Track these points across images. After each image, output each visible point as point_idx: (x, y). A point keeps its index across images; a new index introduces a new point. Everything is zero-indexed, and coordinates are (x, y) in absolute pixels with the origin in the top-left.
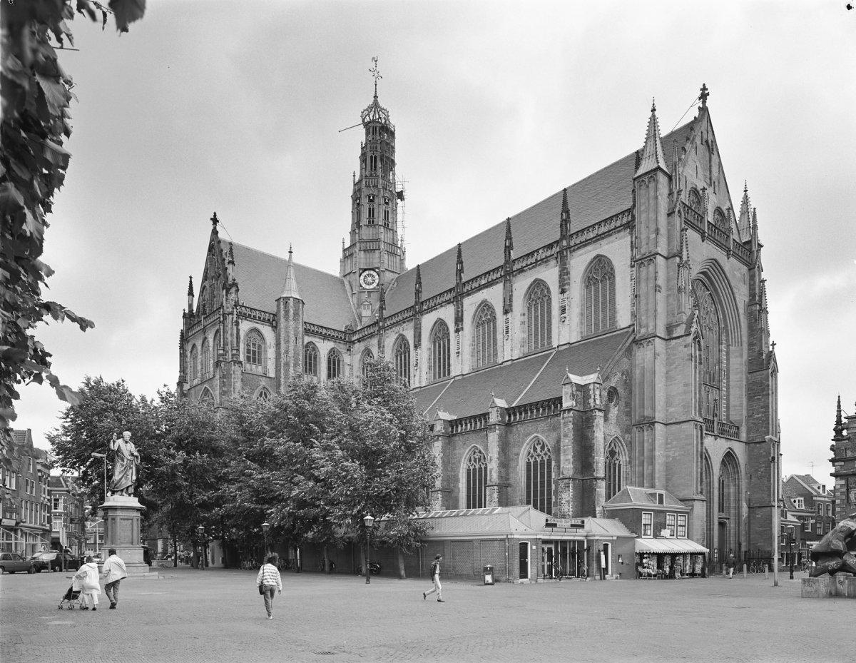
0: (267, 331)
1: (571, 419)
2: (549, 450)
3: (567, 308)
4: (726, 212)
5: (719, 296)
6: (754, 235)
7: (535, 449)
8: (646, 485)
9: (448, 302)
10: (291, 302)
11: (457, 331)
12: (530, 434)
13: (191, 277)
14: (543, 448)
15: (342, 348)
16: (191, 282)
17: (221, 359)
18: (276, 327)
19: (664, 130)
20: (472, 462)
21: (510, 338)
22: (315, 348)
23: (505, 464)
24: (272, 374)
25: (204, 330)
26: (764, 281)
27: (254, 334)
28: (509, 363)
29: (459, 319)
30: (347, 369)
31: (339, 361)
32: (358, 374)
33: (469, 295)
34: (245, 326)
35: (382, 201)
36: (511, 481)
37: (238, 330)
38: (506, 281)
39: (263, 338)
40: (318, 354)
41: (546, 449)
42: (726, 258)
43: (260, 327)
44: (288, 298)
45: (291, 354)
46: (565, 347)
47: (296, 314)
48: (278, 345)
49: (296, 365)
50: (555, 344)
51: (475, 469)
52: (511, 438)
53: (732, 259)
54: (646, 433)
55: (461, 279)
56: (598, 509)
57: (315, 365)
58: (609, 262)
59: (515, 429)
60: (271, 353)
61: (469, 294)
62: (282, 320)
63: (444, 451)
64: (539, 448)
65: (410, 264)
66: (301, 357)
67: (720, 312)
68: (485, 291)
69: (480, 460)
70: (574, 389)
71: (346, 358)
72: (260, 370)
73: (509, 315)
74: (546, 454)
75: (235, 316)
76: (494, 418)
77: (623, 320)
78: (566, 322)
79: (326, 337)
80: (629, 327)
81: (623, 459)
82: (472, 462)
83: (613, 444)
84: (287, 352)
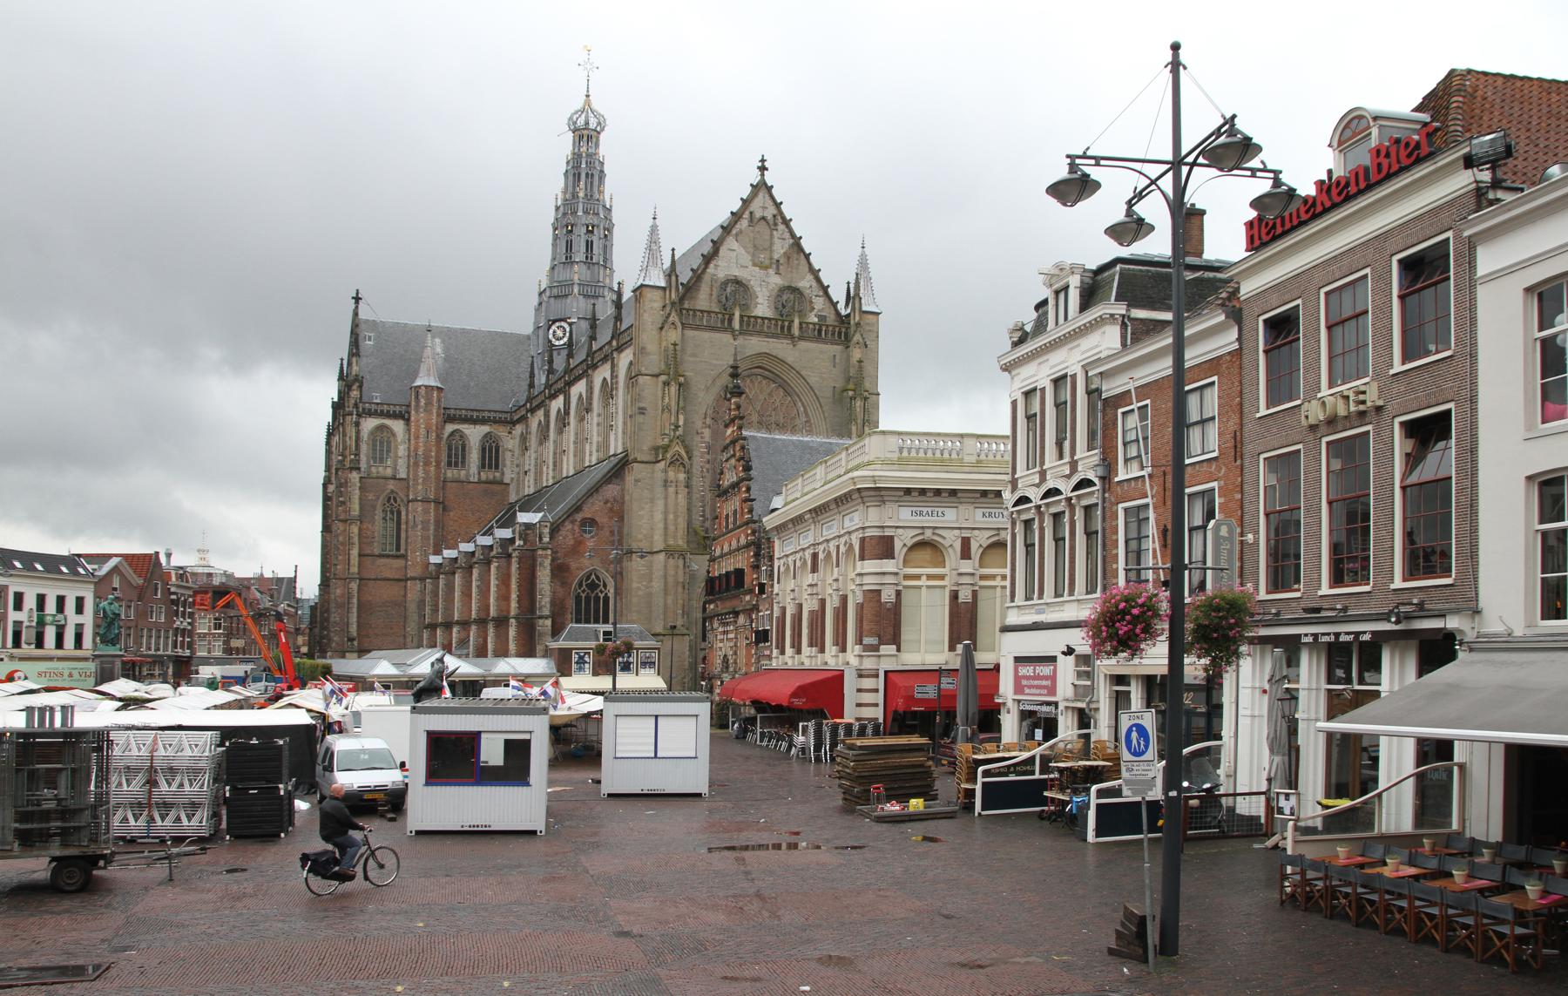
0: (397, 426)
10: (422, 391)
15: (501, 431)
22: (462, 436)
34: (369, 424)
35: (584, 230)
37: (358, 433)
39: (394, 435)
43: (388, 422)
47: (429, 403)
49: (427, 464)
53: (803, 345)
57: (464, 457)
60: (402, 451)
72: (389, 472)
84: (416, 449)
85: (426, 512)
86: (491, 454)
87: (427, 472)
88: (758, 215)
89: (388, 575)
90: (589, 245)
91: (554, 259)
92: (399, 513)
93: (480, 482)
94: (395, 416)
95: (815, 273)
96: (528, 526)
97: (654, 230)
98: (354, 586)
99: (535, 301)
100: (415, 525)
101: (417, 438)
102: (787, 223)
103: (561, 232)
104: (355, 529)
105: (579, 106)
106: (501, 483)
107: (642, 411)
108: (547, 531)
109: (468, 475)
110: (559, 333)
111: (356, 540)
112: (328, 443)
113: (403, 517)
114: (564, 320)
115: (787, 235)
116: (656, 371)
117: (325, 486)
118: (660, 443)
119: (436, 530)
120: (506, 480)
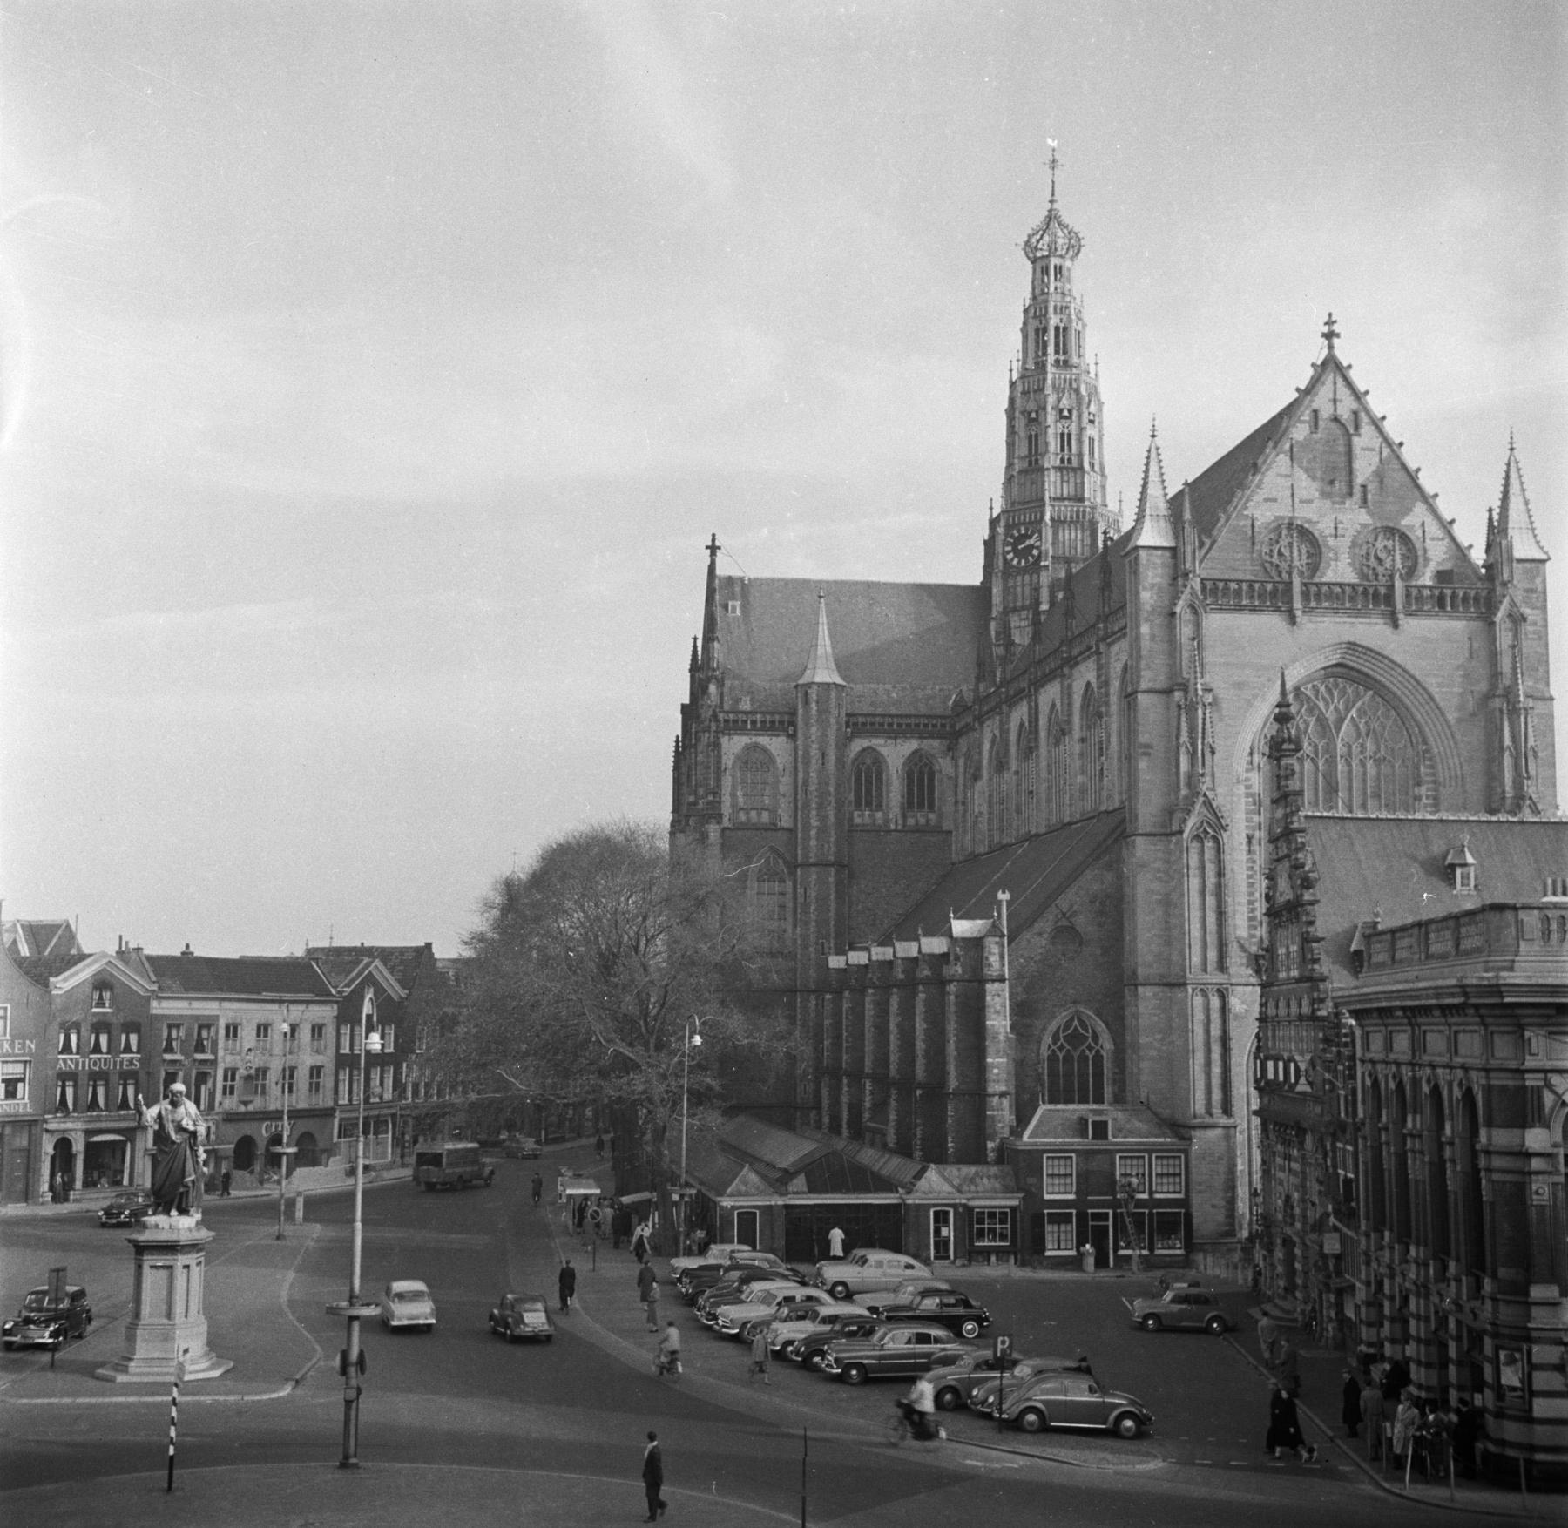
0: (777, 745)
13: (695, 639)
16: (695, 647)
22: (879, 761)
34: (733, 745)
39: (772, 759)
42: (1388, 630)
43: (763, 740)
49: (820, 806)
53: (1410, 625)
56: (990, 1145)
57: (879, 789)
66: (831, 789)
83: (1076, 1023)
84: (806, 782)
87: (823, 818)
88: (1326, 412)
91: (1010, 466)
93: (906, 830)
94: (771, 728)
95: (1428, 501)
102: (1377, 424)
103: (1020, 424)
106: (938, 830)
109: (887, 821)
115: (1377, 442)
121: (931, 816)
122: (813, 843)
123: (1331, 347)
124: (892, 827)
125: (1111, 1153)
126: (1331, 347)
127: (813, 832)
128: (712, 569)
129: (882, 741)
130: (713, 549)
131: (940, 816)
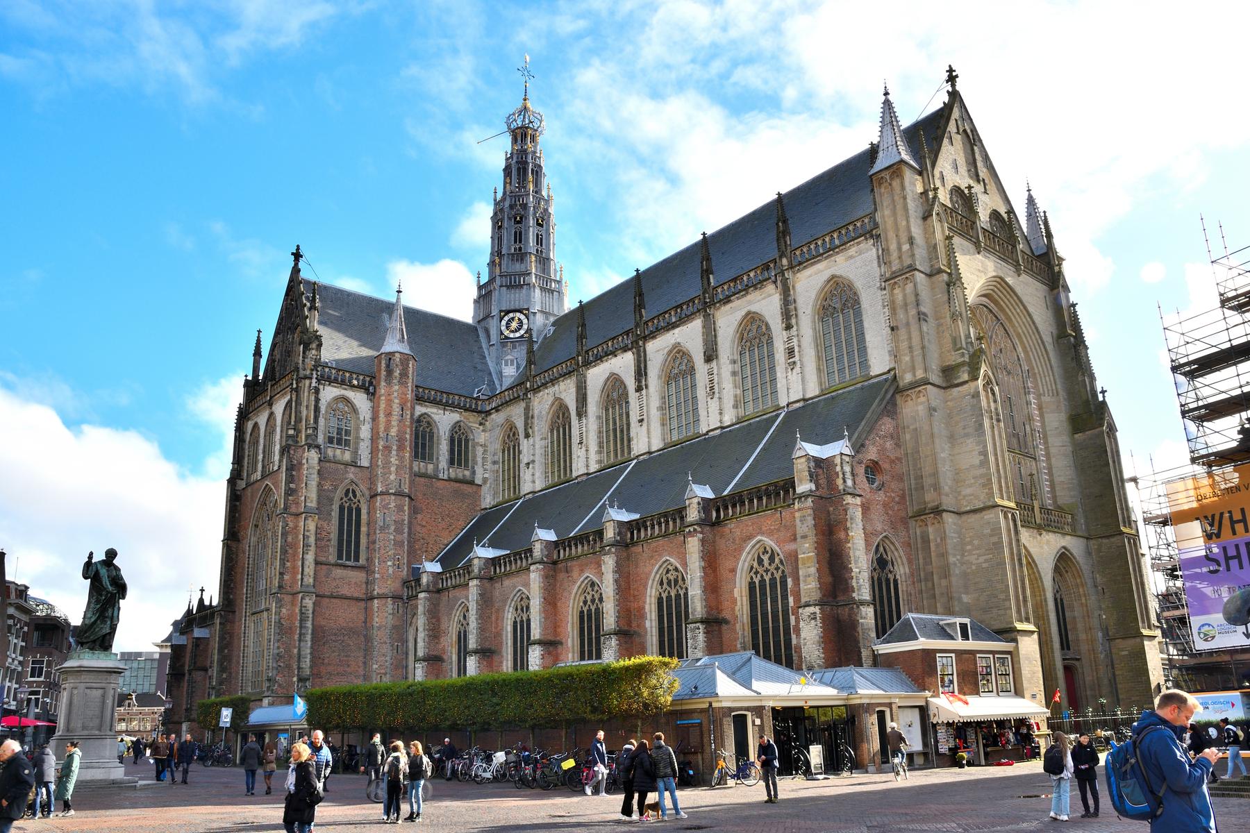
1: (810, 512)
2: (781, 562)
3: (796, 349)
4: (1005, 216)
5: (1013, 326)
6: (1050, 246)
7: (760, 562)
8: (939, 610)
9: (625, 349)
11: (639, 389)
12: (750, 538)
13: (259, 332)
14: (772, 559)
15: (472, 420)
17: (290, 442)
18: (373, 394)
19: (906, 119)
20: (665, 586)
21: (717, 395)
23: (713, 587)
24: (365, 462)
25: (270, 405)
26: (1074, 305)
27: (341, 406)
28: (718, 432)
29: (641, 372)
30: (480, 450)
31: (467, 441)
32: (496, 458)
33: (654, 337)
34: (329, 393)
36: (726, 614)
37: (317, 400)
38: (707, 316)
39: (355, 410)
40: (435, 431)
41: (777, 560)
43: (350, 394)
44: (393, 353)
45: (393, 432)
46: (798, 405)
47: (404, 374)
48: (375, 418)
49: (401, 448)
50: (783, 403)
51: (669, 598)
52: (722, 544)
54: (930, 529)
55: (641, 316)
57: (431, 447)
58: (850, 286)
59: (727, 530)
60: (365, 432)
61: (652, 336)
62: (383, 384)
63: (619, 569)
64: (766, 558)
65: (570, 303)
67: (1020, 349)
68: (677, 331)
69: (676, 581)
70: (812, 464)
71: (481, 437)
72: (347, 456)
73: (714, 364)
74: (777, 569)
75: (314, 381)
76: (693, 514)
77: (879, 363)
78: (797, 369)
79: (446, 406)
80: (889, 371)
81: (901, 571)
82: (665, 586)
83: (881, 549)
85: (400, 508)
86: (460, 447)
87: (401, 458)
89: (345, 591)
90: (539, 240)
92: (359, 510)
93: (450, 480)
96: (818, 462)
97: (888, 105)
98: (309, 603)
99: (474, 293)
100: (384, 528)
101: (389, 415)
104: (312, 526)
105: (519, 105)
106: (471, 483)
107: (921, 317)
108: (847, 469)
109: (436, 468)
110: (514, 325)
111: (312, 540)
112: (240, 428)
113: (364, 516)
114: (520, 311)
116: (928, 271)
117: (232, 482)
118: (954, 358)
119: (409, 534)
120: (478, 481)
121: (467, 473)
122: (392, 477)
123: (953, 85)
124: (441, 476)
125: (973, 653)
126: (953, 85)
127: (393, 469)
128: (296, 270)
129: (435, 410)
130: (297, 256)
131: (474, 473)
